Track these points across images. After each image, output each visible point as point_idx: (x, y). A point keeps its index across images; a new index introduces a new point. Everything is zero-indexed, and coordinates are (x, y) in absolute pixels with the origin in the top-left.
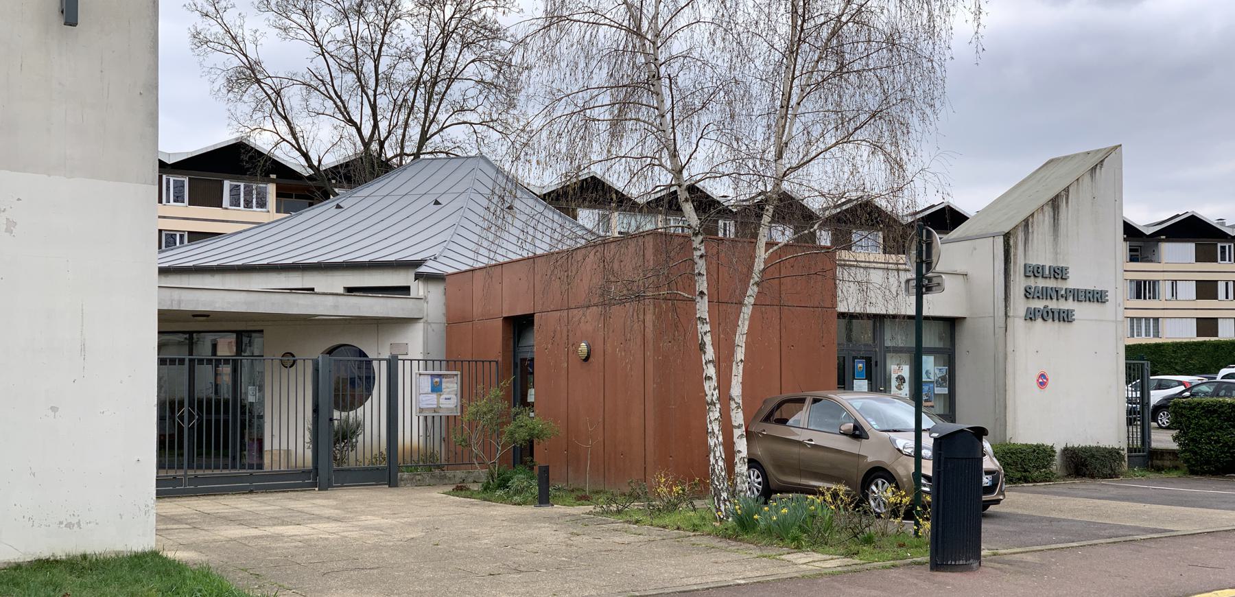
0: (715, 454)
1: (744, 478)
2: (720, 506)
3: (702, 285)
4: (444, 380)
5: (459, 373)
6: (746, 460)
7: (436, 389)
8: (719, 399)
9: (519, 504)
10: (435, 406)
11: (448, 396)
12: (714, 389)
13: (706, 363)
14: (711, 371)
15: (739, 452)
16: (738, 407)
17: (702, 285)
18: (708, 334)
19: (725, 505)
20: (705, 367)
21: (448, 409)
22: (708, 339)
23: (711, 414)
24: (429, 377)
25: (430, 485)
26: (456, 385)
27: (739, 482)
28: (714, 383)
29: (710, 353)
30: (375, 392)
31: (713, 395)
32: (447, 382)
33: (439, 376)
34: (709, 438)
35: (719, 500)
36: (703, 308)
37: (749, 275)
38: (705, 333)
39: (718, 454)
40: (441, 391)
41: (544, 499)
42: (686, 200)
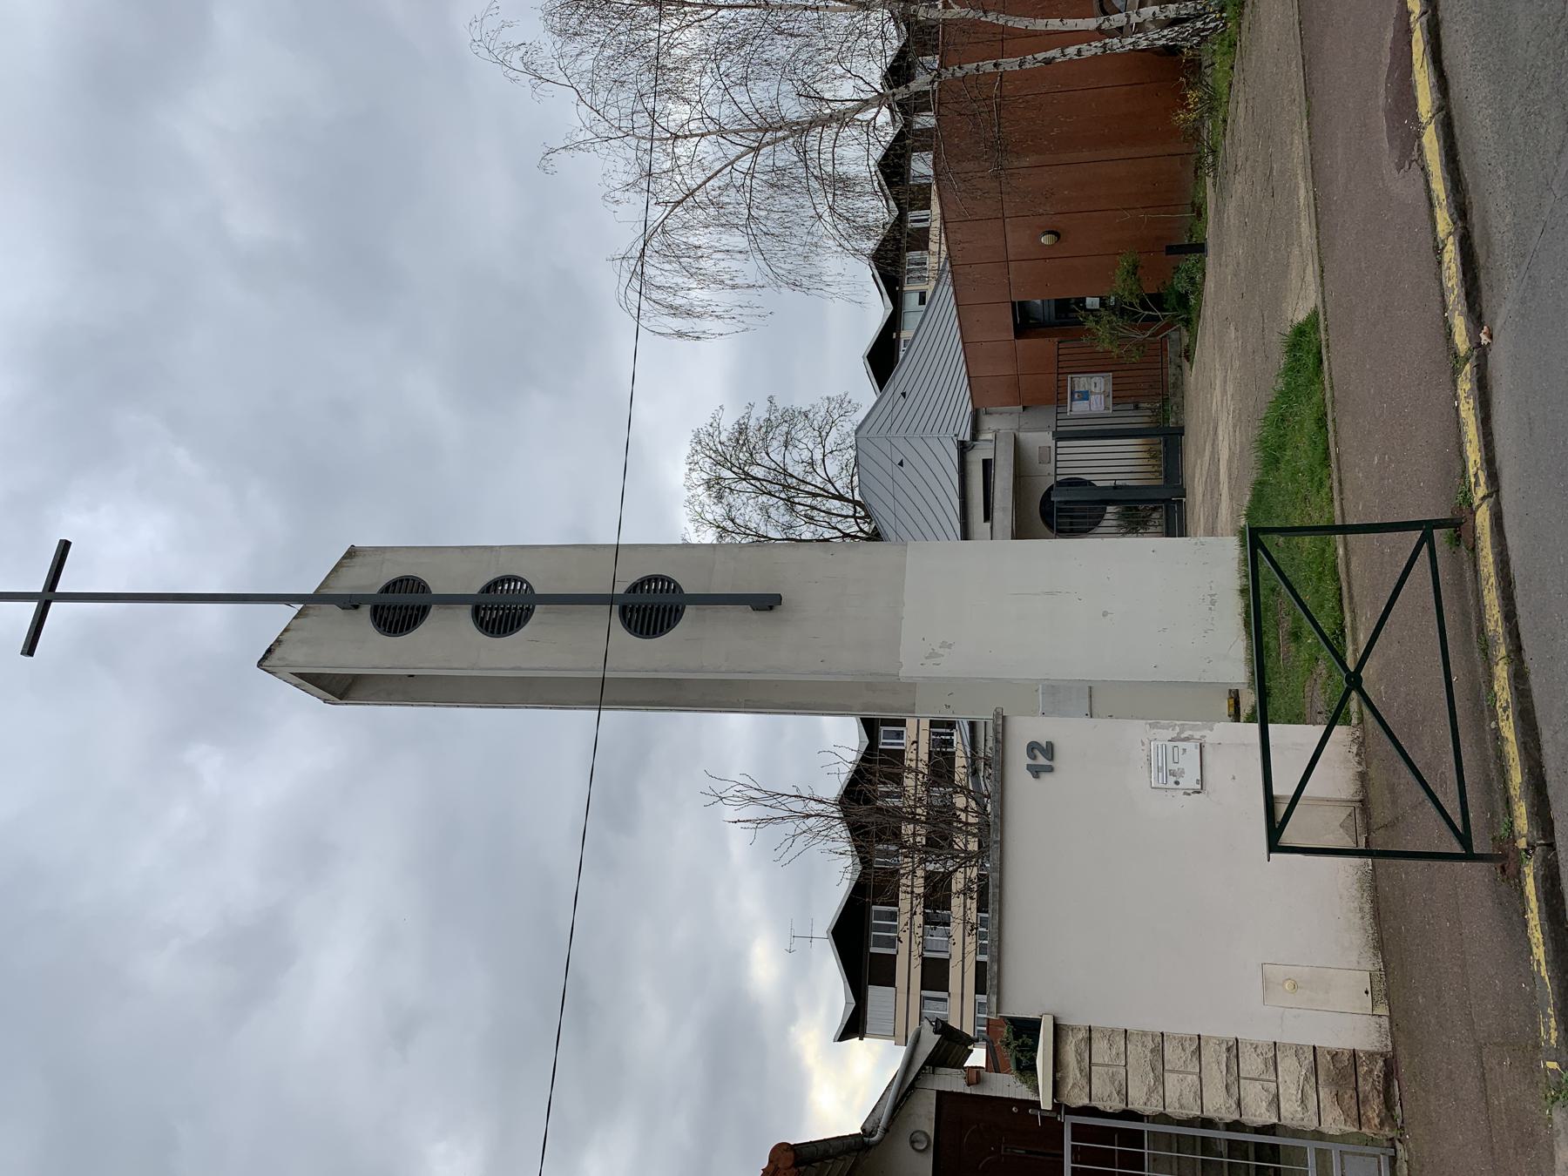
0: (1156, 40)
1: (1181, 6)
2: (1211, 28)
3: (988, 66)
4: (1076, 390)
5: (1070, 376)
6: (1163, 6)
7: (1085, 396)
8: (1100, 41)
9: (1204, 275)
10: (1103, 397)
11: (1093, 385)
12: (1090, 45)
13: (1064, 56)
14: (1071, 51)
15: (1154, 14)
16: (1109, 20)
17: (988, 66)
18: (1036, 56)
19: (1209, 23)
20: (1068, 57)
21: (1105, 385)
22: (1040, 56)
23: (1115, 47)
24: (1074, 403)
25: (1183, 397)
26: (1082, 379)
27: (1185, 12)
28: (1084, 46)
29: (1055, 53)
30: (1087, 478)
31: (1096, 47)
32: (1079, 387)
33: (1072, 393)
34: (1140, 48)
35: (1204, 30)
36: (1010, 64)
37: (976, 23)
38: (1035, 59)
39: (1156, 36)
40: (1087, 391)
41: (1200, 248)
42: (907, 87)
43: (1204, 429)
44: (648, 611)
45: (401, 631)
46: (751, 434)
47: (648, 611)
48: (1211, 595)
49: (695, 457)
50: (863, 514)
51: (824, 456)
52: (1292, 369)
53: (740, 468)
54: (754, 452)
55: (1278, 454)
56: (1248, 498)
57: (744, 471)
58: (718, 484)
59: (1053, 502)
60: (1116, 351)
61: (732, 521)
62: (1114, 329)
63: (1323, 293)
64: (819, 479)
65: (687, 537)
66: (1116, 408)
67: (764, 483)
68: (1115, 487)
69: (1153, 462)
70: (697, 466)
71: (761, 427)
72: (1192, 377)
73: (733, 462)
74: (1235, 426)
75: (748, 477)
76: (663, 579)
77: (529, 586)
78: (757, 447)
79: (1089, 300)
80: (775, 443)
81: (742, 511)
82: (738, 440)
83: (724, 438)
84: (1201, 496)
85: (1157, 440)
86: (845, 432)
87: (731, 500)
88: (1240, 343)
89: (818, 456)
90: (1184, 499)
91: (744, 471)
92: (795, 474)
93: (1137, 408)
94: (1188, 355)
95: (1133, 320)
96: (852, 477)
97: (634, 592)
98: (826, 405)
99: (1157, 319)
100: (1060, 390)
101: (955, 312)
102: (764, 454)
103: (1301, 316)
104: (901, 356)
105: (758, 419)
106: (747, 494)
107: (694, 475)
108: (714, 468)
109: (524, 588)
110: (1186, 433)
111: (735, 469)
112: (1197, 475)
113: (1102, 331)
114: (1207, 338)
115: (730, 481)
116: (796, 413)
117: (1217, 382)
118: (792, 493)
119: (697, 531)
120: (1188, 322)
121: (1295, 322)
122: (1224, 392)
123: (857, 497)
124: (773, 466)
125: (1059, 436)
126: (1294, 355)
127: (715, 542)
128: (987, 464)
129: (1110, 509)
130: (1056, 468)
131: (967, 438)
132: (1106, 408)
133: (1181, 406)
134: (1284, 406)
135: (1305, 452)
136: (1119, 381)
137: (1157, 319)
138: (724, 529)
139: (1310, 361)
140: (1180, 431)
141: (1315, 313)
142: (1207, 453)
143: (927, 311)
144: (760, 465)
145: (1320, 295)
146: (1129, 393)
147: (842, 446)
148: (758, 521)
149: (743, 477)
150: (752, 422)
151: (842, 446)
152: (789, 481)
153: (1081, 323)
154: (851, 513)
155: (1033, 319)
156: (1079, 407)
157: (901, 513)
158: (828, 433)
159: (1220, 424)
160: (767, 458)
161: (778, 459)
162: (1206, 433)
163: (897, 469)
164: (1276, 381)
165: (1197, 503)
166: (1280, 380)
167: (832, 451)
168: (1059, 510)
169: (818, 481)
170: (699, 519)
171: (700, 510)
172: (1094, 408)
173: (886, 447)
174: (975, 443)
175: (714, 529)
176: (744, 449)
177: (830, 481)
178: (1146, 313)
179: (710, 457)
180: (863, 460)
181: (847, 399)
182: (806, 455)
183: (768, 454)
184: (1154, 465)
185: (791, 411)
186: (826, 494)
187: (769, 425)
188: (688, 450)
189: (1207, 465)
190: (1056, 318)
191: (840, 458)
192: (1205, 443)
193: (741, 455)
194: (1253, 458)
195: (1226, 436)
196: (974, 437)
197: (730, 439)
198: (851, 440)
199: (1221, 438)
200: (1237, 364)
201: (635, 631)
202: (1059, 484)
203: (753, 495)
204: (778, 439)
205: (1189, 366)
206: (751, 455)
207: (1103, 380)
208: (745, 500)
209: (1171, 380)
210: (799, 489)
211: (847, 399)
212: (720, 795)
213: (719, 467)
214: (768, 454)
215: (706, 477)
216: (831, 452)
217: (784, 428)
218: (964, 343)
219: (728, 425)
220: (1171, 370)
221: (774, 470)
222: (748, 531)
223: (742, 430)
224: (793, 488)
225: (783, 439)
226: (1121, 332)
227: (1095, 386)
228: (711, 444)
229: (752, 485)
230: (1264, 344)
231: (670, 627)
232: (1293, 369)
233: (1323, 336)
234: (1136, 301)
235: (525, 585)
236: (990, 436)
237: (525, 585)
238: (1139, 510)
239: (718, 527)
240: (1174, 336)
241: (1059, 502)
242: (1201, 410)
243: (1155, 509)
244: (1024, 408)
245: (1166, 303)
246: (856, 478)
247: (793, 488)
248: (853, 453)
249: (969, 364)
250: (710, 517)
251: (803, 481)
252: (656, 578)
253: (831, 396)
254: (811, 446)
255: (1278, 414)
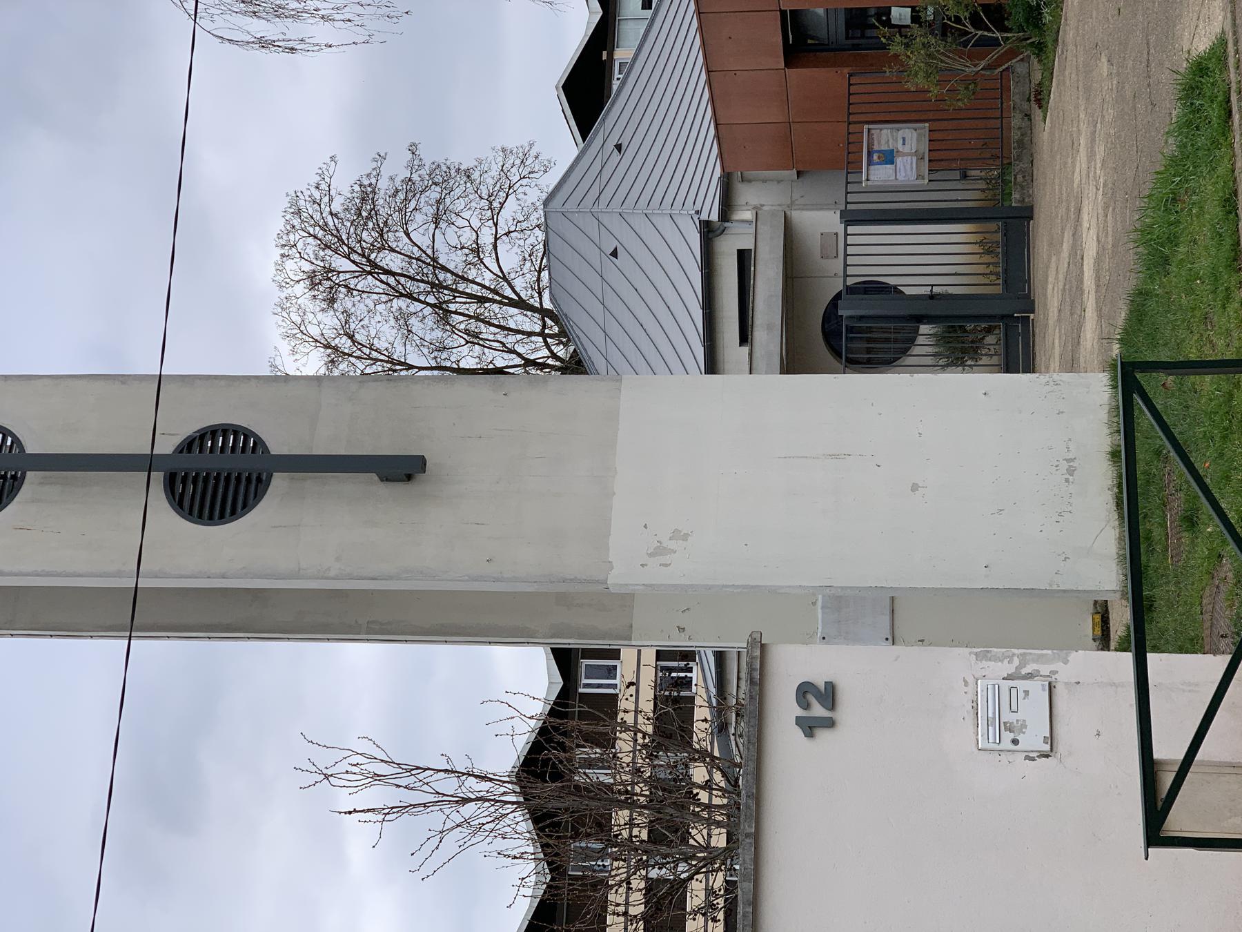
4: (876, 148)
5: (866, 126)
7: (889, 158)
10: (915, 159)
11: (900, 142)
21: (918, 140)
24: (872, 167)
25: (1032, 162)
26: (884, 132)
32: (879, 142)
33: (870, 154)
43: (1062, 211)
44: (212, 482)
45: (222, 516)
46: (381, 202)
47: (212, 482)
48: (1068, 460)
49: (291, 236)
50: (556, 329)
51: (496, 239)
52: (1189, 124)
53: (363, 256)
54: (385, 230)
55: (1166, 251)
56: (1123, 315)
57: (369, 260)
58: (329, 279)
59: (842, 316)
60: (935, 90)
61: (351, 337)
62: (930, 56)
63: (1233, 12)
64: (488, 275)
65: (278, 362)
66: (934, 177)
67: (402, 280)
68: (932, 297)
69: (987, 259)
70: (294, 250)
71: (397, 191)
72: (1047, 133)
73: (353, 245)
74: (1106, 208)
75: (375, 269)
76: (236, 431)
77: (16, 440)
78: (390, 222)
79: (895, 12)
80: (419, 218)
81: (366, 322)
82: (359, 210)
83: (337, 207)
84: (1056, 310)
85: (992, 226)
86: (529, 203)
87: (349, 304)
88: (1115, 82)
89: (486, 238)
90: (1032, 316)
91: (369, 260)
92: (451, 267)
93: (964, 176)
94: (1040, 98)
95: (960, 44)
96: (539, 272)
97: (189, 451)
98: (500, 160)
99: (995, 43)
100: (852, 148)
101: (695, 24)
102: (401, 234)
103: (1203, 46)
104: (615, 87)
105: (392, 179)
106: (375, 297)
107: (290, 264)
108: (322, 253)
109: (9, 443)
110: (1035, 216)
111: (355, 257)
112: (1051, 279)
113: (915, 60)
114: (1067, 73)
115: (348, 276)
116: (453, 172)
117: (1082, 141)
118: (446, 295)
119: (294, 352)
120: (1040, 49)
121: (1194, 53)
122: (1091, 157)
123: (547, 304)
124: (417, 253)
125: (850, 218)
126: (1192, 104)
127: (323, 371)
128: (744, 258)
129: (924, 329)
130: (846, 265)
131: (715, 217)
132: (920, 177)
133: (1029, 177)
134: (1178, 179)
135: (1206, 248)
136: (937, 136)
137: (995, 43)
138: (336, 349)
139: (1214, 112)
140: (1026, 214)
141: (1222, 42)
142: (1066, 247)
143: (653, 19)
144: (393, 250)
145: (1229, 15)
146: (954, 154)
147: (524, 225)
148: (391, 340)
149: (368, 269)
150: (383, 185)
151: (524, 225)
152: (441, 276)
153: (883, 47)
154: (538, 329)
155: (812, 38)
156: (880, 175)
157: (614, 329)
158: (502, 205)
159: (1085, 202)
160: (406, 240)
161: (424, 242)
162: (1065, 217)
163: (607, 262)
164: (1166, 142)
165: (1051, 322)
166: (1171, 141)
167: (510, 232)
168: (851, 330)
169: (487, 278)
170: (299, 332)
171: (298, 320)
172: (901, 177)
173: (591, 227)
174: (727, 224)
175: (322, 350)
176: (370, 225)
177: (505, 278)
178: (980, 33)
179: (315, 237)
180: (555, 244)
181: (533, 152)
182: (468, 237)
183: (407, 234)
184: (988, 264)
185: (444, 168)
186: (497, 298)
187: (410, 190)
188: (280, 225)
189: (1066, 265)
190: (847, 38)
191: (521, 242)
192: (1063, 230)
193: (365, 235)
194: (1131, 256)
195: (1094, 221)
196: (725, 214)
197: (347, 210)
198: (537, 217)
199: (1086, 225)
200: (1110, 114)
201: (191, 513)
202: (851, 290)
203: (384, 298)
204: (424, 210)
205: (1041, 114)
206: (381, 235)
207: (915, 134)
208: (372, 305)
209: (1015, 135)
210: (456, 291)
211: (533, 152)
212: (325, 771)
213: (330, 253)
214: (407, 234)
215: (307, 267)
216: (507, 234)
217: (434, 194)
218: (708, 72)
219: (344, 185)
220: (1016, 121)
221: (418, 259)
222: (374, 354)
223: (367, 194)
224: (446, 288)
225: (431, 211)
226: (942, 61)
227: (904, 144)
228: (317, 216)
229: (382, 281)
230: (1149, 85)
231: (247, 507)
232: (1190, 124)
233: (1232, 75)
234: (964, 15)
235: (9, 440)
236: (748, 215)
237: (9, 440)
238: (965, 331)
239: (327, 346)
240: (1021, 69)
241: (851, 317)
242: (1057, 181)
243: (989, 330)
244: (799, 174)
245: (1008, 19)
246: (545, 275)
247: (446, 288)
248: (540, 235)
249: (717, 105)
250: (314, 331)
251: (463, 278)
252: (225, 430)
253: (509, 146)
254: (476, 223)
255: (1168, 190)
